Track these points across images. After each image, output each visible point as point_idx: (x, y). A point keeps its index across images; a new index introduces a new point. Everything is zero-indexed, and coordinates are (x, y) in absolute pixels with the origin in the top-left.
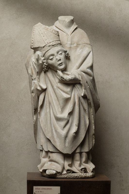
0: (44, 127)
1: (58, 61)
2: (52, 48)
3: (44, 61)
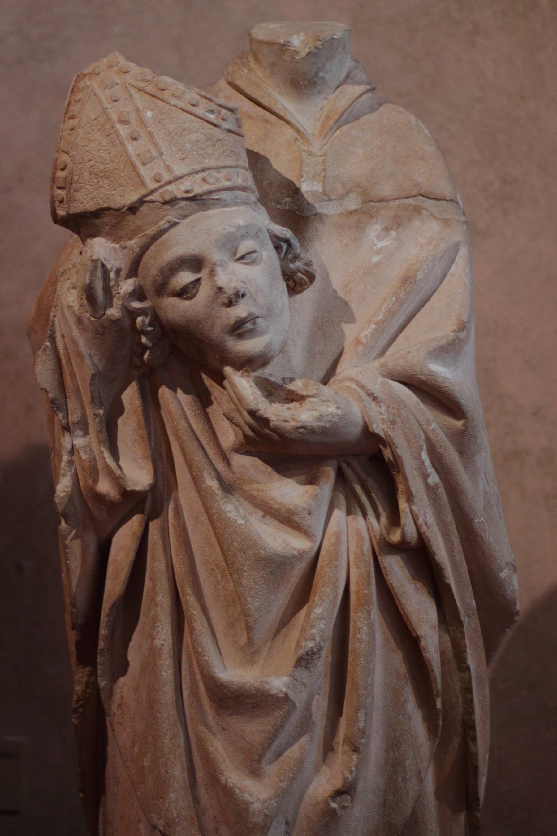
0: (136, 750)
1: (230, 304)
2: (185, 216)
3: (136, 305)
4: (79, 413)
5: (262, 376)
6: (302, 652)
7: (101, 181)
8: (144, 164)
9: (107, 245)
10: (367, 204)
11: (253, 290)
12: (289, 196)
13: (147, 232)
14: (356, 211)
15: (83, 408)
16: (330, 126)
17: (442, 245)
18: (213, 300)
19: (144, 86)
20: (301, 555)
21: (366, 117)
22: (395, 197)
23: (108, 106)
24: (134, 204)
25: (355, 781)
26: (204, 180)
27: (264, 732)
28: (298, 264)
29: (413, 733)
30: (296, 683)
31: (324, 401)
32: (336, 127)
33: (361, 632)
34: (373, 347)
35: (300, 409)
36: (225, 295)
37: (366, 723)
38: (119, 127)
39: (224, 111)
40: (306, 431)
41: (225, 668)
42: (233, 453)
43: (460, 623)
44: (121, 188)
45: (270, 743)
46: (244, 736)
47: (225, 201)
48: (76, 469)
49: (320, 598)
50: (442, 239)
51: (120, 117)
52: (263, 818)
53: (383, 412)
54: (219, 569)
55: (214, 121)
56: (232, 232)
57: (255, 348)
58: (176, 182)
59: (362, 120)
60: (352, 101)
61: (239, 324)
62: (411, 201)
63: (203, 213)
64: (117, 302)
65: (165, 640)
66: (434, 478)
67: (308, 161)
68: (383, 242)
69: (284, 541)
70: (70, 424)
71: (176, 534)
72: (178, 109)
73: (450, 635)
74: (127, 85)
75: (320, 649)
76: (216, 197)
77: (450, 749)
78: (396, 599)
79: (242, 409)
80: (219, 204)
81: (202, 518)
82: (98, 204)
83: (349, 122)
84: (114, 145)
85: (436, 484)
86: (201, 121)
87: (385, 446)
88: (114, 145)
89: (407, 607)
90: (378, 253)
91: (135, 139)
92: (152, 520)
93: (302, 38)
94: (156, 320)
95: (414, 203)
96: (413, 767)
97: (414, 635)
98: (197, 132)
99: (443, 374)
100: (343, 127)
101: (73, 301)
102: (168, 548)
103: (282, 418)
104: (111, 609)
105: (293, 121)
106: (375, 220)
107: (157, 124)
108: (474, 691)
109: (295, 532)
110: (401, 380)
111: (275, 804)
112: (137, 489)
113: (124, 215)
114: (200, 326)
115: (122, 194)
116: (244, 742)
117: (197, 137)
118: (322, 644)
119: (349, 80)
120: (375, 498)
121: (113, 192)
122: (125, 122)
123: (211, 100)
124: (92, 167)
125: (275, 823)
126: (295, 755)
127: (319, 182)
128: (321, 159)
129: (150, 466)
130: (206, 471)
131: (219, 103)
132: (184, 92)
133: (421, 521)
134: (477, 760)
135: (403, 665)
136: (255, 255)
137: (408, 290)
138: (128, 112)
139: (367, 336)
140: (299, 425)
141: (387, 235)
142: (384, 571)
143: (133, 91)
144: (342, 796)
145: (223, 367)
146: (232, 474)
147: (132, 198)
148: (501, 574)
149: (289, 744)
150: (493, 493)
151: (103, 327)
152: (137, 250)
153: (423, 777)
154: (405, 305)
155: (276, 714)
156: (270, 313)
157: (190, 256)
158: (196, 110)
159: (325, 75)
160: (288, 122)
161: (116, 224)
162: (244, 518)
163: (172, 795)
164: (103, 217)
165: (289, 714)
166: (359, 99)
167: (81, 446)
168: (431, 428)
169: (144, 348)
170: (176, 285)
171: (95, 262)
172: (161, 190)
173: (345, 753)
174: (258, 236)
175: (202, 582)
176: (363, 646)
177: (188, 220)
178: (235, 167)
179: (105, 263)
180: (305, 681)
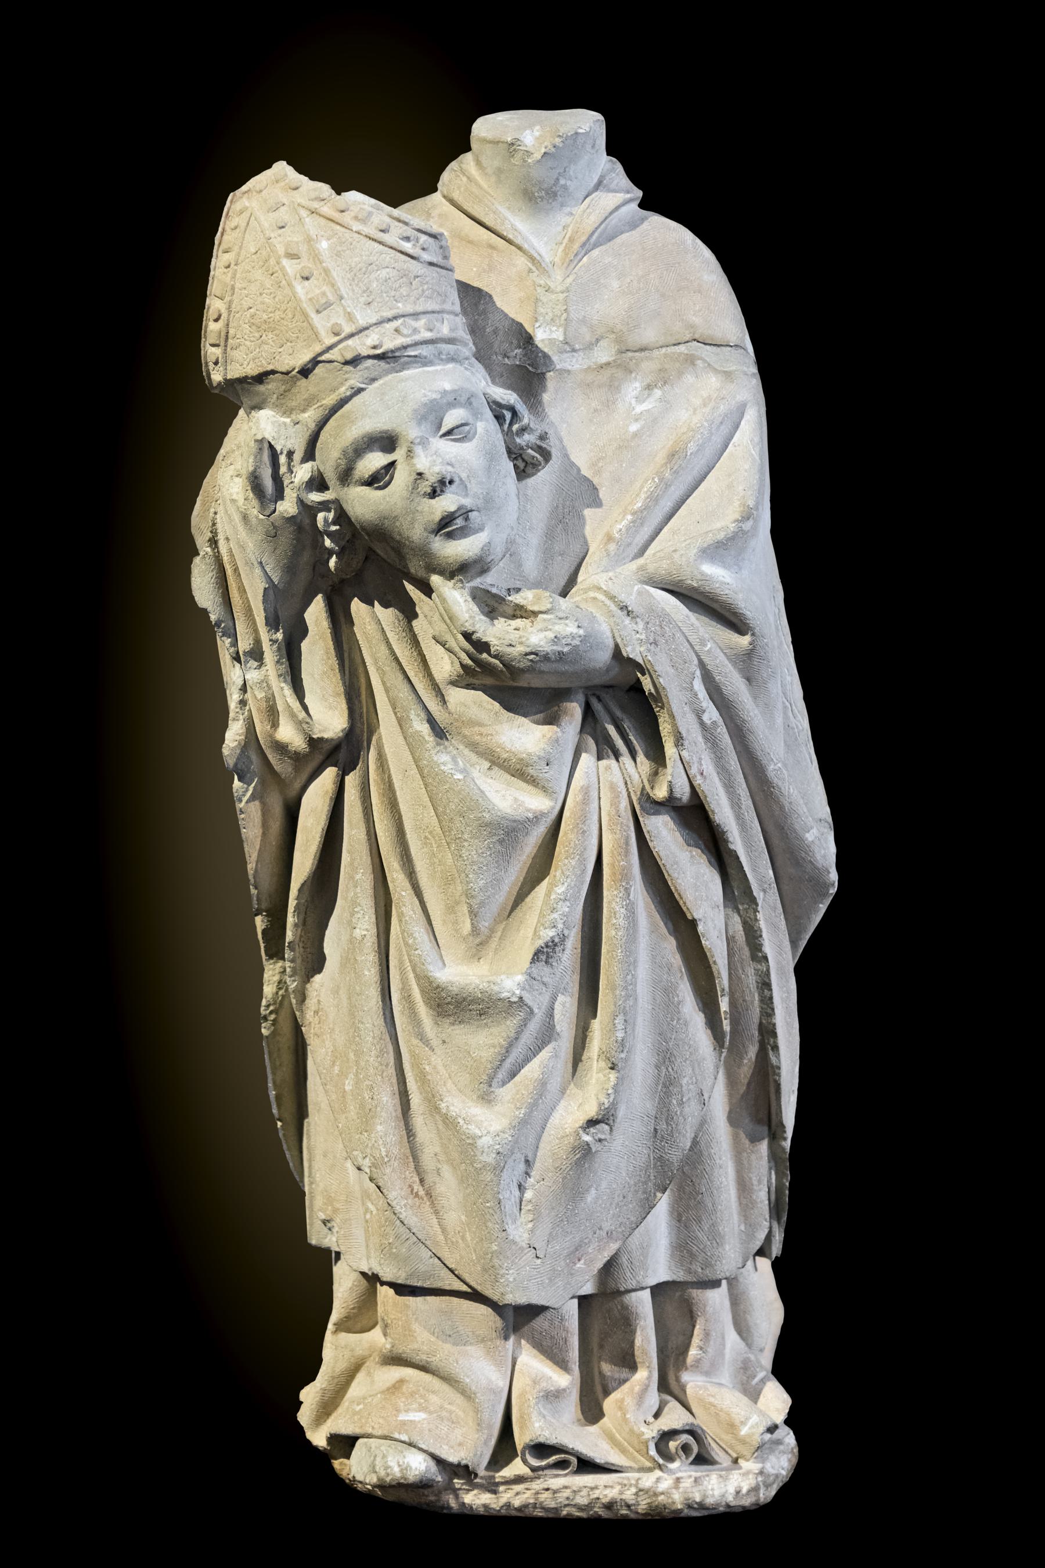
0: (336, 1069)
1: (433, 494)
2: (373, 380)
3: (315, 497)
4: (251, 638)
5: (481, 586)
6: (540, 943)
7: (264, 336)
8: (318, 312)
9: (275, 419)
10: (623, 355)
11: (464, 475)
12: (520, 348)
13: (324, 402)
14: (608, 364)
15: (256, 631)
16: (575, 252)
17: (722, 407)
18: (413, 489)
19: (317, 207)
20: (537, 818)
21: (624, 236)
22: (661, 343)
23: (272, 235)
24: (305, 365)
25: (614, 1105)
26: (397, 330)
27: (494, 1047)
28: (527, 437)
29: (691, 1043)
30: (534, 982)
31: (560, 619)
32: (583, 252)
33: (618, 916)
34: (629, 545)
35: (530, 629)
36: (427, 482)
37: (626, 1032)
38: (285, 262)
39: (423, 238)
40: (538, 658)
41: (444, 964)
42: (450, 686)
43: (753, 901)
44: (289, 344)
45: (502, 1061)
46: (469, 1052)
47: (426, 358)
48: (250, 710)
49: (563, 873)
50: (723, 398)
51: (286, 250)
52: (494, 1156)
53: (640, 631)
54: (434, 837)
55: (411, 251)
56: (435, 399)
57: (469, 551)
58: (360, 335)
59: (618, 240)
60: (604, 216)
61: (447, 520)
62: (682, 348)
63: (396, 374)
64: (290, 495)
65: (367, 930)
66: (712, 714)
67: (545, 300)
68: (644, 404)
69: (516, 800)
70: (241, 653)
71: (379, 793)
72: (362, 237)
73: (741, 916)
74: (296, 206)
75: (564, 938)
76: (413, 353)
77: (745, 1061)
78: (664, 872)
79: (455, 632)
80: (416, 362)
81: (412, 772)
82: (261, 366)
83: (601, 245)
84: (280, 287)
85: (714, 723)
86: (394, 251)
87: (643, 674)
88: (280, 287)
89: (679, 881)
90: (636, 420)
91: (307, 279)
92: (348, 774)
93: (537, 134)
94: (342, 517)
95: (686, 352)
96: (691, 1087)
97: (690, 918)
98: (387, 267)
99: (721, 578)
100: (593, 251)
101: (238, 493)
102: (369, 810)
103: (507, 642)
104: (300, 890)
105: (526, 246)
106: (633, 375)
107: (335, 257)
108: (774, 986)
109: (530, 787)
110: (671, 588)
111: (510, 1139)
112: (326, 736)
113: (294, 381)
114: (398, 524)
115: (291, 352)
116: (469, 1059)
117: (388, 273)
118: (566, 932)
119: (601, 188)
120: (635, 742)
121: (280, 350)
122: (293, 256)
123: (406, 224)
124: (252, 316)
125: (510, 1162)
126: (536, 1076)
127: (558, 327)
128: (562, 296)
129: (344, 706)
130: (413, 712)
131: (418, 227)
132: (370, 214)
133: (694, 771)
134: (779, 1075)
135: (678, 956)
136: (467, 428)
137: (675, 469)
138: (297, 243)
139: (621, 530)
140: (528, 650)
141: (649, 395)
142: (647, 837)
143: (304, 213)
144: (597, 1126)
145: (430, 576)
146: (447, 714)
147: (304, 357)
148: (807, 835)
149: (527, 1060)
150: (801, 728)
151: (275, 527)
152: (312, 426)
153: (706, 1099)
154: (673, 488)
155: (508, 1022)
156: (489, 503)
157: (381, 432)
158: (385, 237)
159: (569, 183)
160: (520, 248)
161: (285, 391)
162: (463, 771)
163: (379, 1128)
164: (268, 383)
165: (525, 1023)
166: (616, 214)
167: (255, 681)
168: (707, 649)
169: (330, 553)
170: (364, 471)
171: (260, 442)
172: (340, 346)
173: (600, 1071)
174: (470, 404)
175: (413, 855)
176: (620, 934)
177: (376, 384)
178: (439, 312)
179: (273, 443)
180: (545, 979)
